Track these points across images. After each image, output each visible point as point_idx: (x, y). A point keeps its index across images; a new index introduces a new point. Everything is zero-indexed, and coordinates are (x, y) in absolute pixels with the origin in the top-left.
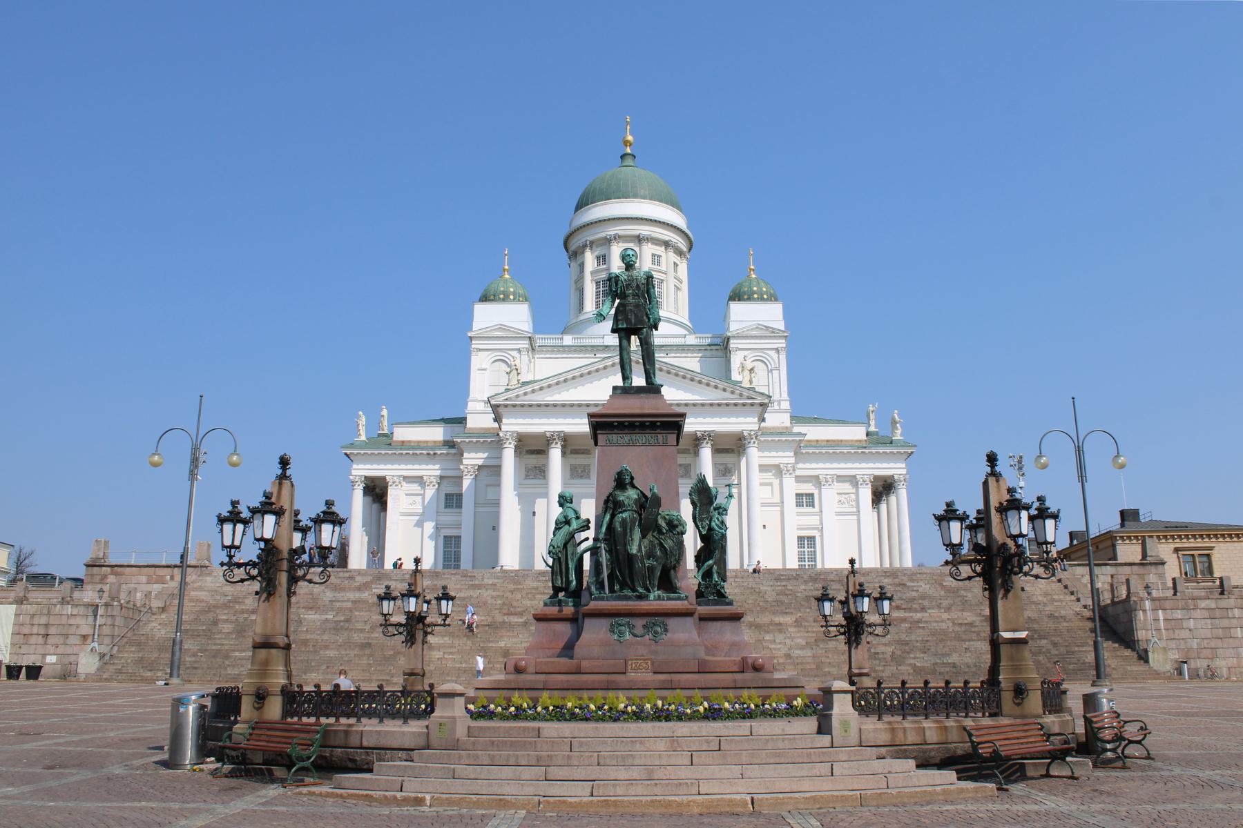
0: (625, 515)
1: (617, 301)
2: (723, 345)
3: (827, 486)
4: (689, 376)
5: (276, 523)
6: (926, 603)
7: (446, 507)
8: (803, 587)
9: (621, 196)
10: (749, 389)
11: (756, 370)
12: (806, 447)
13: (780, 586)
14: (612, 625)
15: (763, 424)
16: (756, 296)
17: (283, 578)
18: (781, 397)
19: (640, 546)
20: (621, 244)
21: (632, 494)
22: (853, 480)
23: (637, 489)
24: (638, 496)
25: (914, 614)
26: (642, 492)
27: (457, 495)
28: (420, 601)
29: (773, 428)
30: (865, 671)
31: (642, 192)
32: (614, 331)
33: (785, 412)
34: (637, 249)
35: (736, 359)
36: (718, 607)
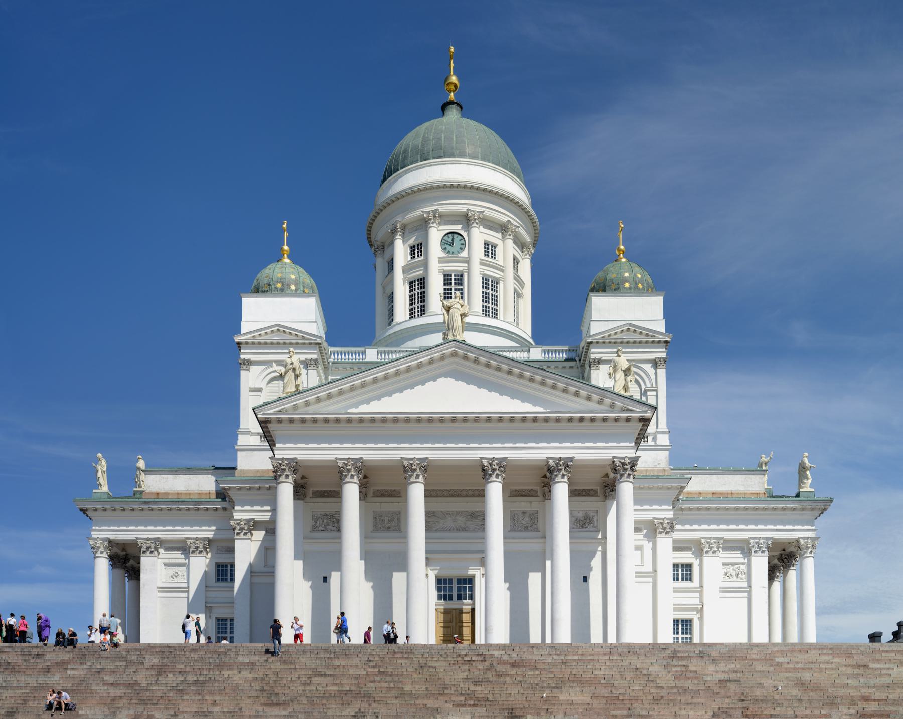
8: (712, 668)
9: (443, 155)
13: (678, 666)
18: (657, 428)
31: (469, 150)
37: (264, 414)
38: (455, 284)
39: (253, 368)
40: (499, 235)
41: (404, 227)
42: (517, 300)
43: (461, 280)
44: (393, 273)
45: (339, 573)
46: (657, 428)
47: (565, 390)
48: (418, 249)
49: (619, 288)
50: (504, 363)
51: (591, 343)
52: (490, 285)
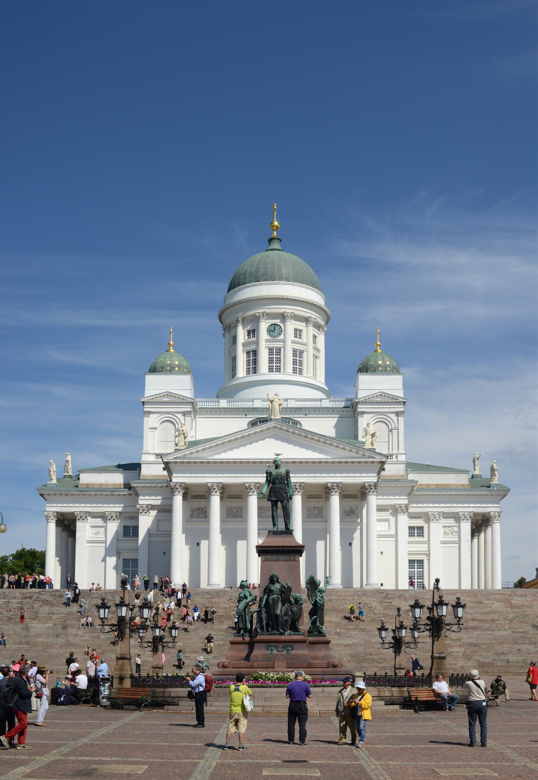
2: (353, 407)
3: (435, 521)
4: (322, 440)
6: (496, 617)
10: (369, 450)
11: (376, 435)
12: (419, 490)
14: (268, 646)
18: (398, 451)
19: (281, 610)
20: (267, 321)
21: (278, 586)
22: (457, 517)
25: (485, 624)
26: (282, 585)
29: (391, 476)
30: (402, 667)
33: (401, 463)
34: (282, 325)
35: (363, 422)
36: (319, 638)
37: (167, 459)
38: (276, 355)
39: (151, 415)
40: (304, 324)
41: (244, 319)
42: (315, 361)
43: (280, 352)
44: (236, 345)
45: (207, 541)
46: (398, 451)
47: (337, 447)
48: (252, 333)
49: (375, 370)
50: (302, 432)
51: (358, 402)
52: (298, 354)
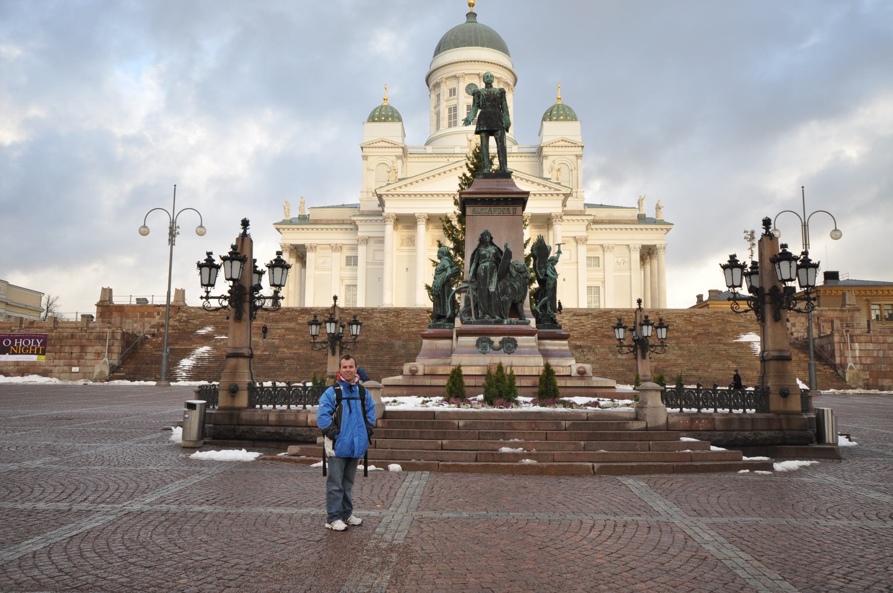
0: (487, 264)
1: (479, 111)
5: (241, 267)
7: (347, 265)
11: (561, 170)
15: (565, 209)
16: (562, 118)
17: (247, 306)
21: (492, 250)
23: (495, 246)
24: (496, 250)
26: (498, 248)
27: (354, 257)
28: (338, 325)
29: (572, 211)
32: (477, 133)
35: (547, 164)
